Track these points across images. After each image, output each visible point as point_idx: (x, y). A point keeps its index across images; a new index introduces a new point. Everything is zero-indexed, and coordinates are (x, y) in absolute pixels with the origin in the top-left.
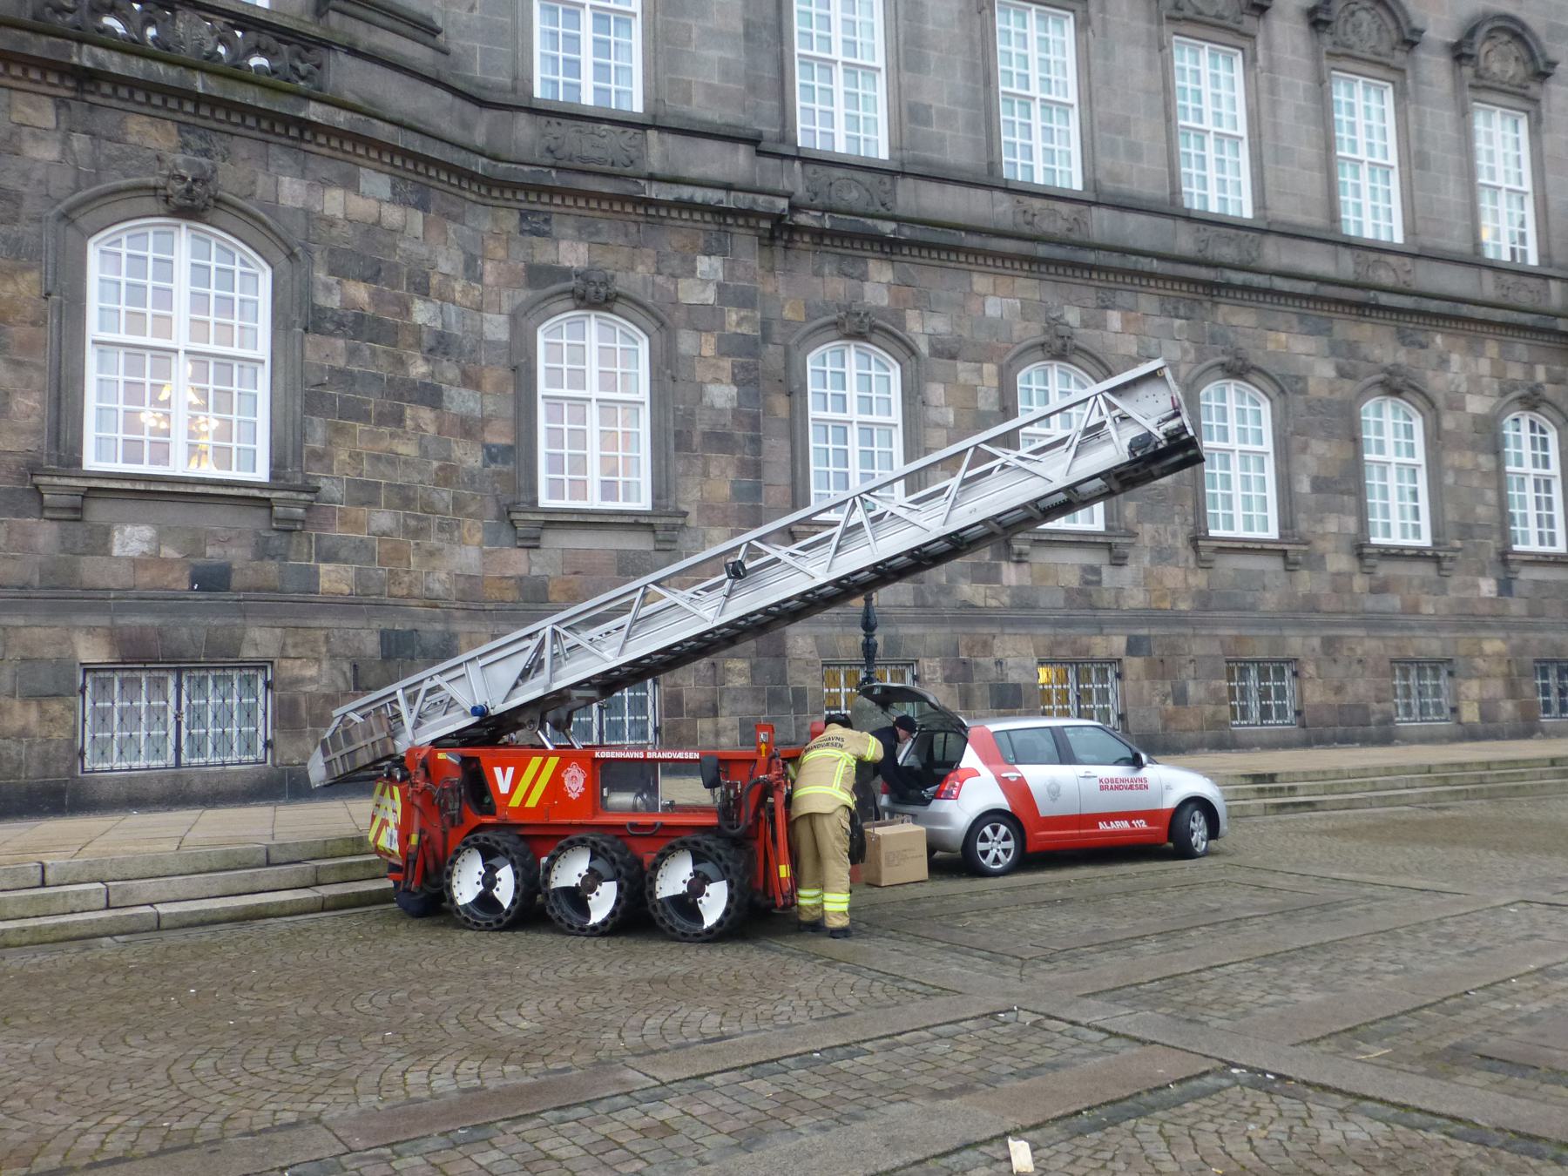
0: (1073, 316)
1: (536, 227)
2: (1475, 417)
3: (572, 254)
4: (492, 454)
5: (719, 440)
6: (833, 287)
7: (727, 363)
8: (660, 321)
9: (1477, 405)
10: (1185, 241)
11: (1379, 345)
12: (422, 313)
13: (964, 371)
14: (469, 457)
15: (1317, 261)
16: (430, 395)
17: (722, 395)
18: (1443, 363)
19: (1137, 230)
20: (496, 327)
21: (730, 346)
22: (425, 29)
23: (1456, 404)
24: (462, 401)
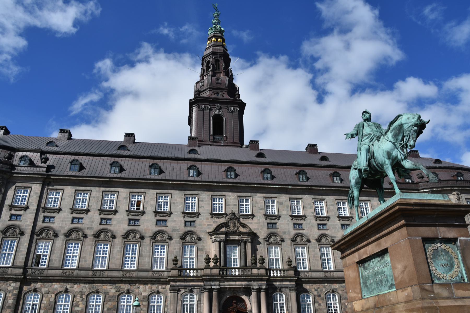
2: (144, 296)
5: (9, 307)
7: (12, 297)
9: (144, 294)
11: (125, 287)
13: (49, 296)
19: (83, 273)
23: (140, 294)
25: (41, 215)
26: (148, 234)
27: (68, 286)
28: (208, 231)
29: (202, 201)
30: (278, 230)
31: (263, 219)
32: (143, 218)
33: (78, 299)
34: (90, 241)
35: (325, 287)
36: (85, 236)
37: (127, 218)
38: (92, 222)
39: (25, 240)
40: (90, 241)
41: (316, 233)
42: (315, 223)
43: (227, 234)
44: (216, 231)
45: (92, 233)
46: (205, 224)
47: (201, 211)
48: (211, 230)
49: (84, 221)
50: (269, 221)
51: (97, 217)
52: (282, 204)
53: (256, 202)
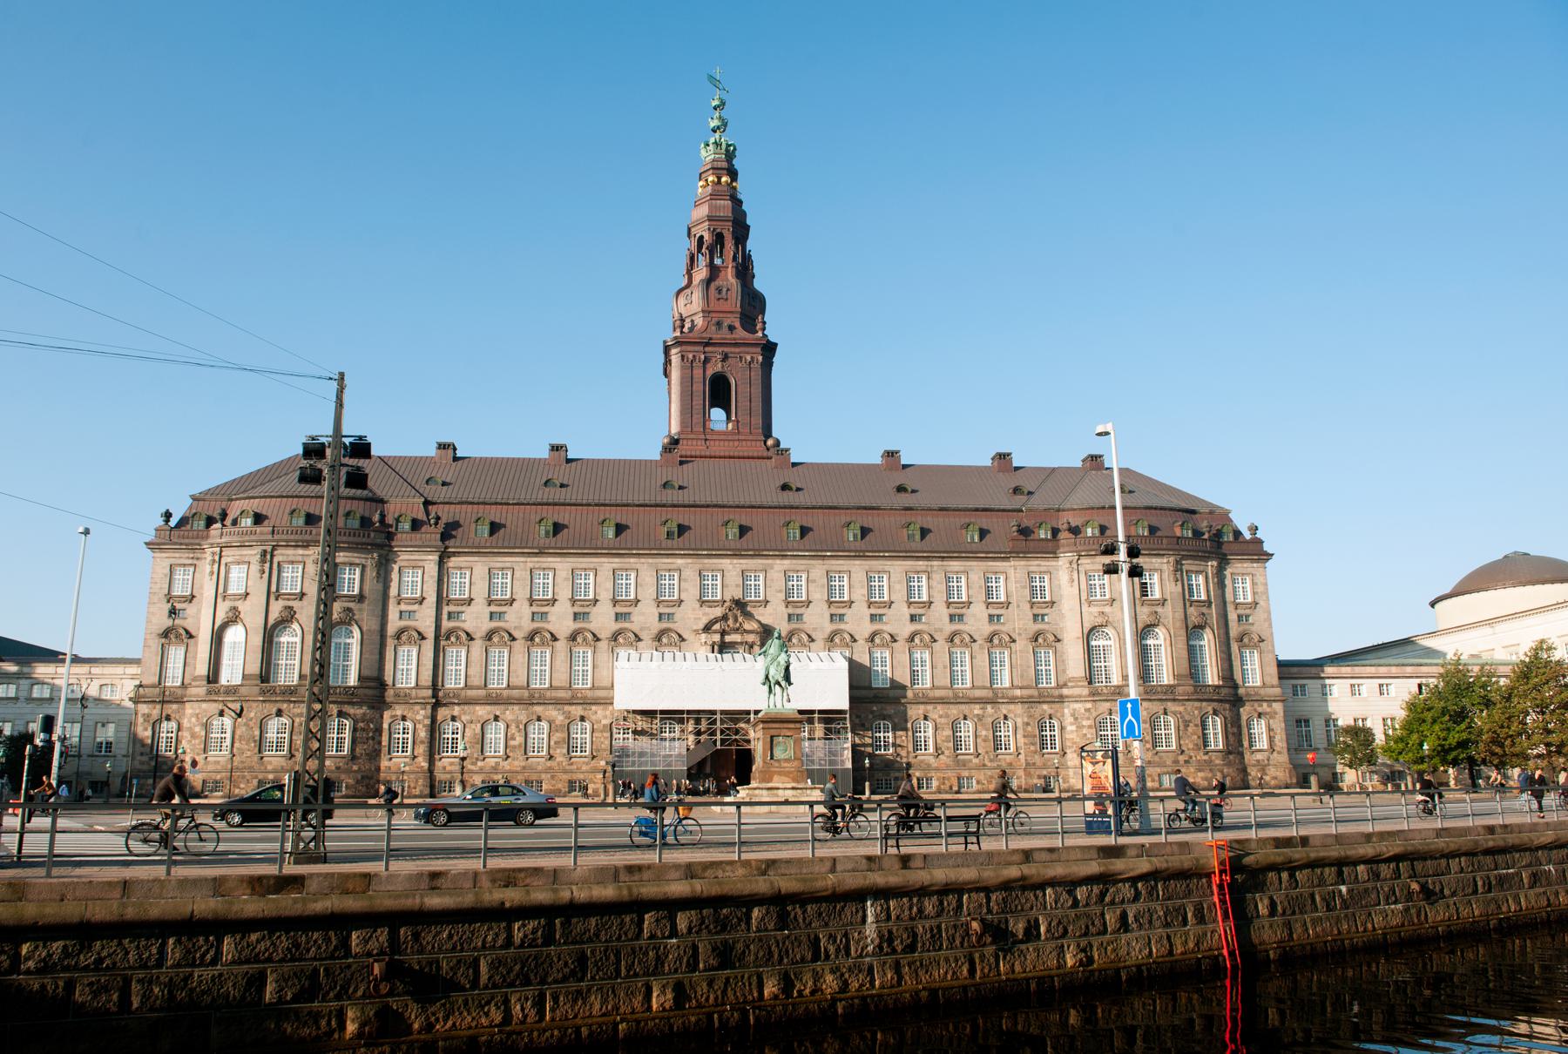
9: (605, 722)
11: (577, 711)
15: (561, 694)
25: (446, 610)
27: (497, 710)
32: (594, 611)
33: (513, 729)
34: (519, 646)
37: (571, 611)
38: (519, 618)
39: (428, 646)
40: (519, 646)
41: (867, 628)
43: (723, 633)
44: (707, 629)
49: (507, 617)
51: (527, 611)
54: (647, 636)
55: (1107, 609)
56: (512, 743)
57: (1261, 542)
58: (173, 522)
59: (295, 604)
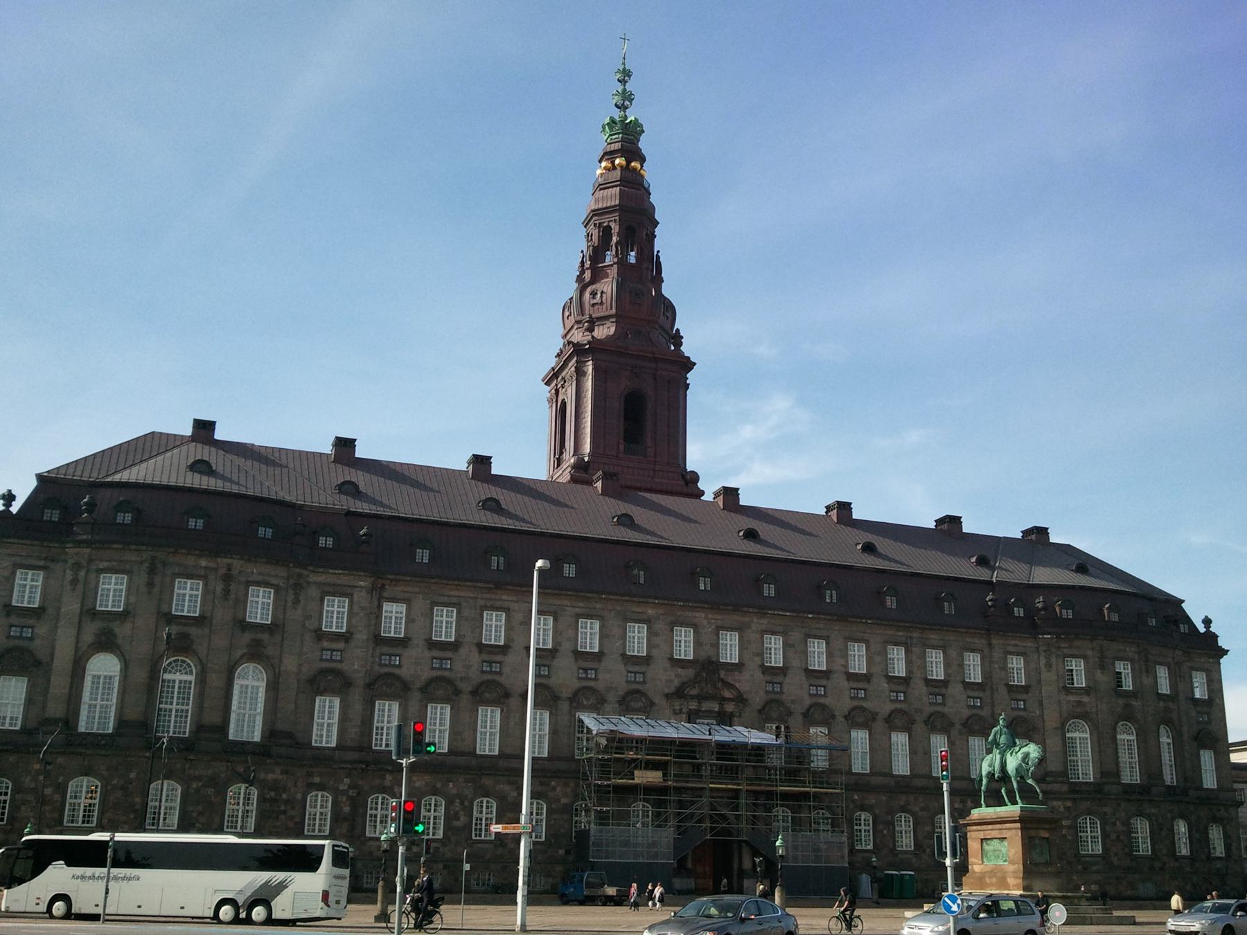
0: (439, 785)
1: (309, 775)
3: (317, 780)
4: (296, 823)
6: (377, 782)
8: (336, 793)
9: (564, 801)
10: (474, 762)
12: (284, 796)
14: (291, 824)
16: (284, 812)
17: (347, 809)
18: (554, 789)
20: (299, 796)
21: (351, 798)
22: (289, 735)
24: (291, 813)
26: (566, 693)
28: (666, 691)
29: (656, 634)
30: (784, 697)
31: (759, 674)
32: (555, 663)
35: (854, 801)
36: (457, 692)
42: (845, 684)
45: (470, 689)
46: (661, 679)
47: (655, 652)
48: (672, 689)
50: (768, 678)
52: (792, 646)
53: (749, 641)
54: (612, 697)
55: (1085, 699)
56: (456, 823)
57: (1215, 637)
58: (15, 508)
59: (193, 631)
